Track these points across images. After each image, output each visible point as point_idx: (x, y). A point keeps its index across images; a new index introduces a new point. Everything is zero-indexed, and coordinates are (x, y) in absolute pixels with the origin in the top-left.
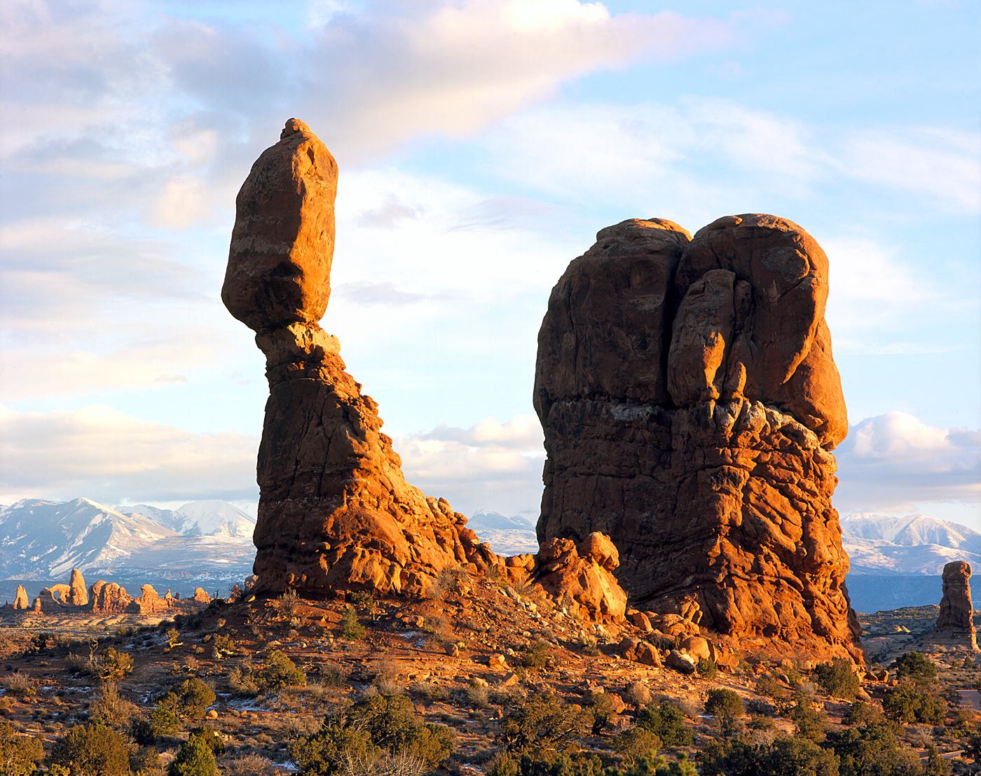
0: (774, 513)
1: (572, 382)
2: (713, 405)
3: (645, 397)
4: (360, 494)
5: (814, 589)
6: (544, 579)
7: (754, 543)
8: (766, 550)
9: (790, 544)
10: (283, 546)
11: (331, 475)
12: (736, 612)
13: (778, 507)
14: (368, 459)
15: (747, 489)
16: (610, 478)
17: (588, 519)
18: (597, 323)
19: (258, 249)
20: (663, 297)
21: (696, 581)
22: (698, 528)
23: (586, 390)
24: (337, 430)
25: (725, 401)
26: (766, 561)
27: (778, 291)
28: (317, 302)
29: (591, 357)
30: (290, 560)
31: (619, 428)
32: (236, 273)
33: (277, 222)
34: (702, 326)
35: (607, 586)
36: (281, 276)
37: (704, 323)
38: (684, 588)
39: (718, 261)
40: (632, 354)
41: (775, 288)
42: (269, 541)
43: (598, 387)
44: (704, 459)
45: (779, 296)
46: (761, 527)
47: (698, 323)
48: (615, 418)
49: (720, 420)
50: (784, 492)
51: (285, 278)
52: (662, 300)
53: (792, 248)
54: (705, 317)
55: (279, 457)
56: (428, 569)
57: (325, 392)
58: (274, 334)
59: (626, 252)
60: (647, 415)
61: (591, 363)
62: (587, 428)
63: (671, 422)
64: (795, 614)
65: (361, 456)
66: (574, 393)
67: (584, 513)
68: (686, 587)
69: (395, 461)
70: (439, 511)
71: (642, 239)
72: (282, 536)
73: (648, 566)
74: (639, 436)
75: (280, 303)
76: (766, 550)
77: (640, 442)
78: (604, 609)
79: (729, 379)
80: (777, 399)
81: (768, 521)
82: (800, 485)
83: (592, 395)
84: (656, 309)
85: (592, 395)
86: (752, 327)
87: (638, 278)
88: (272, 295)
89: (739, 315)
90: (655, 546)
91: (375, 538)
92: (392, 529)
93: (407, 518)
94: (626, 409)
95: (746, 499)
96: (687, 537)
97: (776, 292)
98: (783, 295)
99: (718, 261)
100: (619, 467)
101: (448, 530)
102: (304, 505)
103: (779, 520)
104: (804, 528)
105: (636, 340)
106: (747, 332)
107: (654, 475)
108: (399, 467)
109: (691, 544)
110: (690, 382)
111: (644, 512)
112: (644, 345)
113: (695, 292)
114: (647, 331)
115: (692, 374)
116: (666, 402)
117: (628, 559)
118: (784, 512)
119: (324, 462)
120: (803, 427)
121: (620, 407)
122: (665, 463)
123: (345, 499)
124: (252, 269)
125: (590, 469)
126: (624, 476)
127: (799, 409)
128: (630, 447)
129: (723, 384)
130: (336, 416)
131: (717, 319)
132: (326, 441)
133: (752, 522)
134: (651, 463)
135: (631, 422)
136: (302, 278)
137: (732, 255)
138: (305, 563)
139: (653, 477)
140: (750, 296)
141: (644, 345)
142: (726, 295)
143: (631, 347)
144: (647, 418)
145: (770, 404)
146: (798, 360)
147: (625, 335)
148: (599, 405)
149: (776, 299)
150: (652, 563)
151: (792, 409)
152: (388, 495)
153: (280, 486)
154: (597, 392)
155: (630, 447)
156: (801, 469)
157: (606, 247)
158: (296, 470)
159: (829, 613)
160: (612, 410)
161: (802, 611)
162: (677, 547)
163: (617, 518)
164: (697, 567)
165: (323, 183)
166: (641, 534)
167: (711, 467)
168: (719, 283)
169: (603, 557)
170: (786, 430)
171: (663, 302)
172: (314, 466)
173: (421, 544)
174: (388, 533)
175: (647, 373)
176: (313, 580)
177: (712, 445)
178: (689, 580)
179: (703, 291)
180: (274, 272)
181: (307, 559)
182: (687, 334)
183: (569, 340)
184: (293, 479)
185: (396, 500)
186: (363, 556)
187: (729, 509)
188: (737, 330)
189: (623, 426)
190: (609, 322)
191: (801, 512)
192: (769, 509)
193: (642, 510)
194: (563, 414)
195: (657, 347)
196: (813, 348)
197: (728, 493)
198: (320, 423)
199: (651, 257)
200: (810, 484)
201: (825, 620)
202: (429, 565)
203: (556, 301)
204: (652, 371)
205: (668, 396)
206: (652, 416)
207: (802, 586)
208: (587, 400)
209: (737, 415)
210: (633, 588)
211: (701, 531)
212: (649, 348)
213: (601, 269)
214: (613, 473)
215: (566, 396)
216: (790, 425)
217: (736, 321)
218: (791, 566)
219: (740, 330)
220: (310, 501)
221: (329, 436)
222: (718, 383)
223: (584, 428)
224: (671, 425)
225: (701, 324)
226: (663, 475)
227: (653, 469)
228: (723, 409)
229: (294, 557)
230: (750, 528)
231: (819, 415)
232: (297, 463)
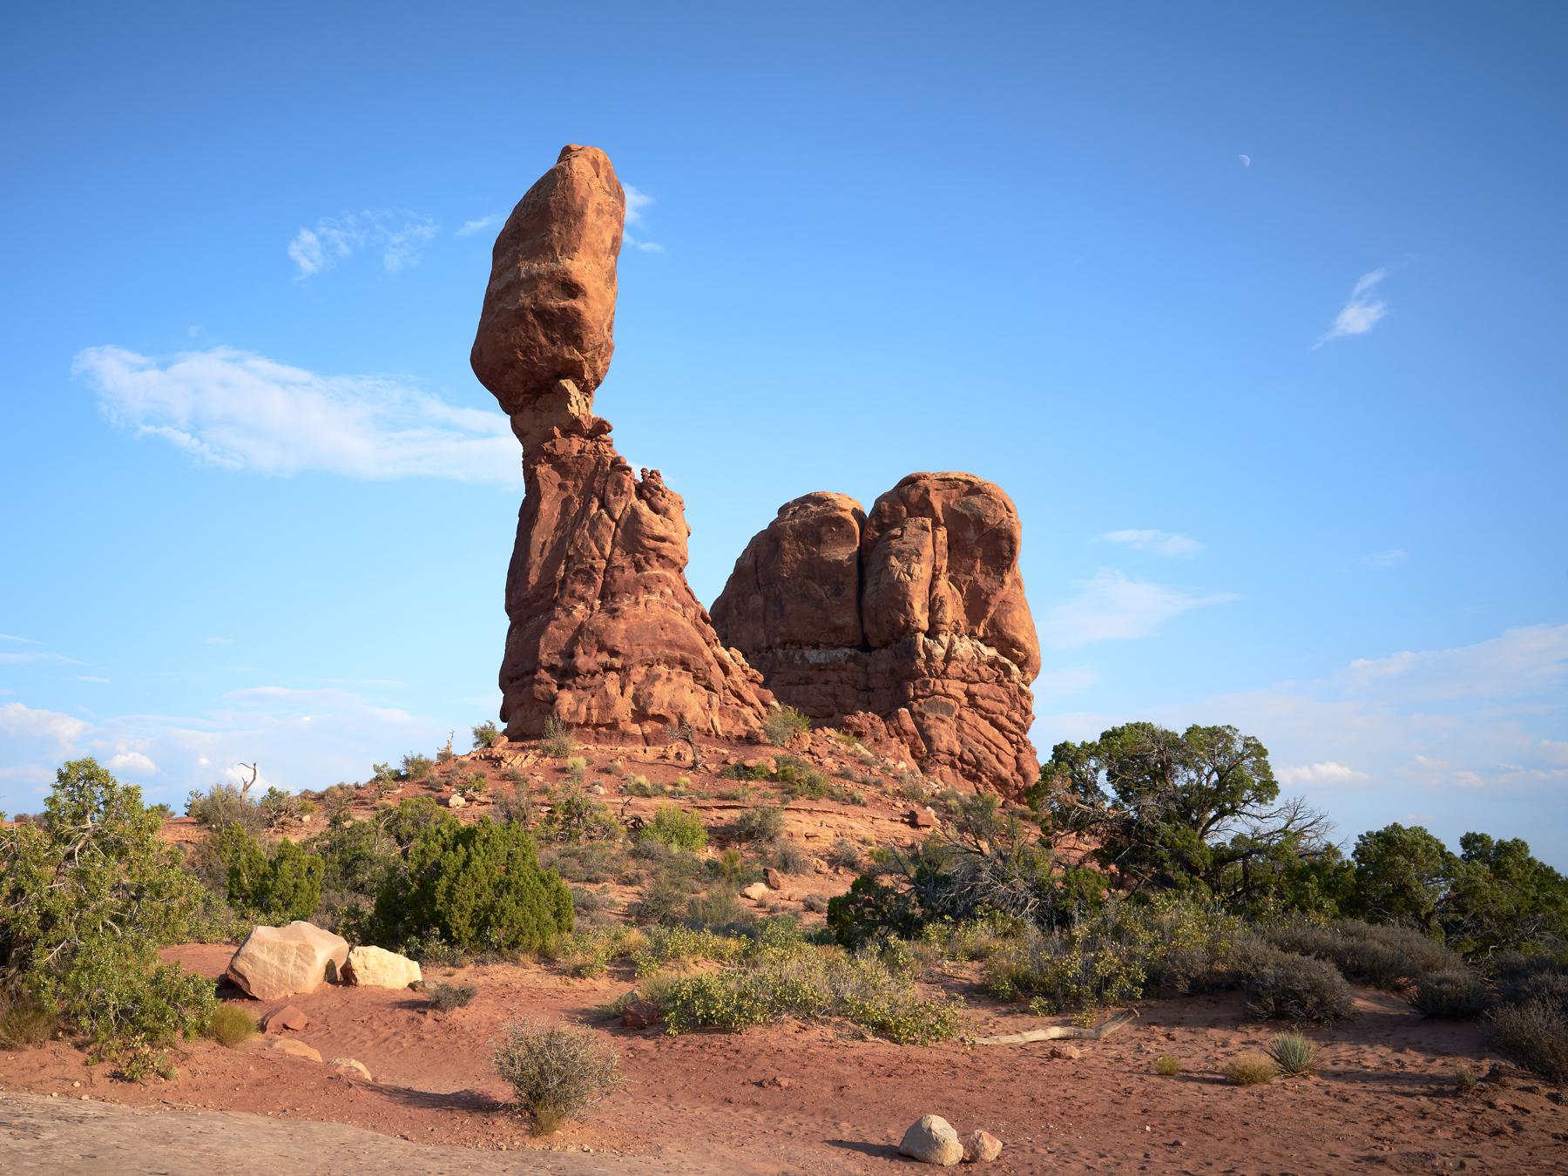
0: (987, 742)
1: (761, 635)
2: (921, 637)
4: (662, 593)
8: (985, 780)
9: (1005, 773)
14: (673, 543)
23: (778, 640)
25: (932, 633)
32: (492, 317)
41: (972, 531)
50: (994, 723)
58: (537, 404)
65: (663, 539)
76: (985, 780)
81: (981, 748)
82: (1008, 717)
83: (783, 645)
85: (783, 645)
91: (686, 654)
95: (960, 729)
103: (994, 749)
104: (1016, 758)
112: (838, 592)
113: (895, 537)
118: (997, 742)
120: (1007, 661)
121: (814, 652)
123: (642, 600)
133: (970, 751)
135: (827, 664)
136: (586, 303)
137: (924, 505)
141: (838, 592)
146: (1001, 594)
147: (816, 586)
148: (791, 653)
153: (542, 596)
156: (1007, 700)
160: (806, 655)
186: (669, 679)
187: (945, 738)
191: (1011, 742)
192: (983, 739)
196: (1013, 585)
197: (943, 721)
200: (1017, 717)
205: (865, 637)
209: (946, 646)
224: (867, 666)
230: (968, 756)
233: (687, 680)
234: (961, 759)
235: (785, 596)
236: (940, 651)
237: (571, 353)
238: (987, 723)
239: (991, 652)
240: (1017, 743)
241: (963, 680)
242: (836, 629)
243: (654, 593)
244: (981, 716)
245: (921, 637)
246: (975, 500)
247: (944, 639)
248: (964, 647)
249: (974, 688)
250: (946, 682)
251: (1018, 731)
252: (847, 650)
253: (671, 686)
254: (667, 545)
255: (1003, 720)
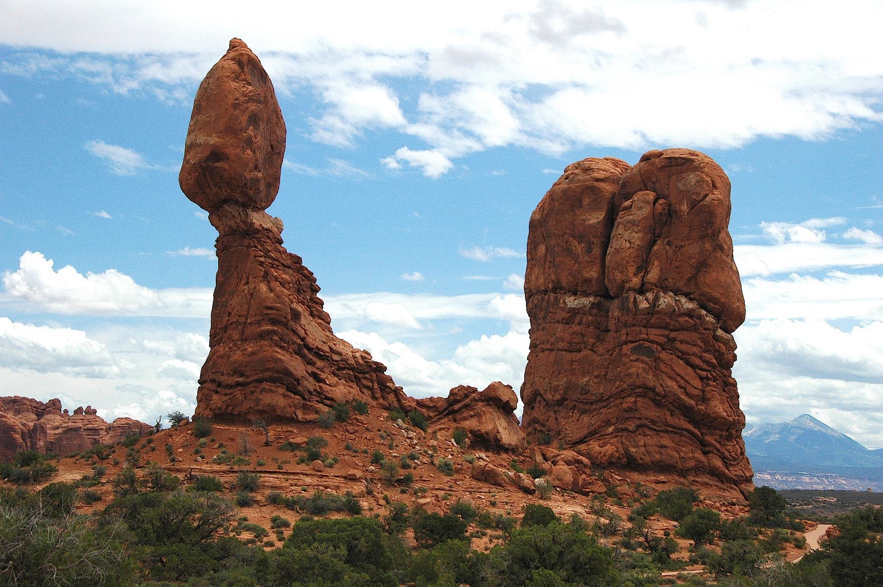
1: (542, 280)
3: (590, 290)
4: (271, 339)
5: (709, 438)
6: (450, 417)
7: (663, 401)
10: (213, 381)
11: (251, 323)
12: (644, 455)
13: (682, 373)
15: (657, 359)
16: (564, 352)
17: (550, 383)
18: (559, 235)
19: (198, 142)
20: (604, 214)
21: (617, 430)
22: (620, 389)
24: (257, 288)
26: (672, 415)
27: (687, 206)
28: (246, 184)
29: (554, 261)
30: (217, 392)
31: (571, 314)
33: (211, 118)
34: (628, 233)
35: (505, 424)
36: (214, 163)
37: (630, 231)
38: (606, 435)
39: (645, 185)
40: (581, 257)
41: (686, 205)
42: (206, 377)
43: (558, 284)
44: (627, 335)
45: (688, 210)
46: (668, 389)
47: (626, 231)
48: (568, 306)
49: (639, 306)
50: (688, 363)
51: (217, 164)
52: (601, 217)
53: (700, 173)
54: (630, 227)
55: (218, 311)
56: (328, 402)
57: (253, 258)
59: (580, 181)
60: (589, 303)
61: (554, 266)
62: (551, 314)
63: (608, 309)
64: (694, 458)
66: (542, 288)
67: (546, 379)
68: (609, 434)
69: (324, 317)
70: (361, 361)
71: (592, 171)
72: (213, 373)
73: (585, 419)
74: (584, 320)
75: (215, 185)
77: (586, 325)
78: (498, 441)
79: (648, 274)
80: (685, 290)
83: (555, 290)
84: (598, 222)
85: (555, 290)
86: (669, 235)
87: (587, 200)
88: (209, 178)
89: (657, 226)
90: (591, 403)
92: (297, 367)
93: (320, 364)
94: (576, 299)
96: (612, 396)
97: (686, 208)
98: (692, 209)
99: (645, 185)
100: (571, 344)
101: (367, 375)
102: (230, 348)
105: (584, 247)
106: (664, 238)
107: (595, 349)
108: (329, 323)
109: (614, 401)
110: (617, 276)
111: (585, 377)
114: (592, 240)
115: (619, 270)
116: (606, 295)
117: (573, 413)
118: (687, 378)
119: (247, 314)
120: (704, 312)
121: (572, 298)
122: (603, 340)
124: (194, 158)
125: (552, 345)
126: (574, 350)
127: (702, 298)
128: (577, 328)
129: (643, 278)
130: (258, 277)
131: (639, 228)
132: (249, 297)
133: (661, 385)
134: (592, 341)
137: (655, 180)
138: (226, 395)
139: (594, 351)
140: (667, 211)
141: (589, 250)
142: (646, 211)
143: (580, 252)
144: (590, 305)
145: (680, 294)
148: (559, 297)
149: (686, 213)
150: (589, 416)
151: (697, 297)
152: (299, 341)
154: (557, 288)
155: (577, 328)
156: (702, 345)
157: (566, 179)
158: (228, 320)
159: (724, 458)
160: (566, 301)
161: (699, 455)
162: (605, 404)
163: (566, 382)
164: (617, 419)
165: (250, 88)
166: (582, 395)
167: (632, 342)
168: (643, 201)
169: (500, 400)
170: (690, 314)
171: (604, 218)
172: (240, 316)
173: (327, 383)
174: (292, 369)
175: (590, 271)
176: (230, 408)
177: (633, 325)
178: (611, 429)
179: (631, 207)
180: (208, 159)
181: (228, 391)
182: (617, 240)
183: (542, 249)
184: (226, 328)
185: (307, 346)
188: (656, 237)
189: (574, 312)
190: (567, 234)
191: (701, 379)
192: (674, 376)
193: (584, 376)
194: (535, 305)
195: (598, 252)
197: (643, 362)
198: (247, 283)
199: (596, 184)
200: (707, 356)
201: (718, 463)
202: (332, 399)
203: (534, 221)
204: (594, 270)
205: (607, 289)
206: (593, 304)
207: (701, 436)
208: (552, 293)
209: (651, 301)
210: (571, 435)
211: (622, 391)
212: (593, 253)
213: (562, 195)
214: (566, 348)
215: (538, 291)
216: (693, 310)
217: (655, 230)
218: (691, 421)
219: (659, 237)
220: (235, 345)
221: (251, 292)
222: (639, 278)
223: (548, 315)
225: (627, 232)
226: (600, 349)
227: (594, 344)
228: (641, 297)
229: (219, 389)
230: (659, 389)
231: (716, 301)
232: (230, 314)
233: (281, 390)
234: (653, 390)
235: (556, 249)
236: (644, 305)
237: (226, 190)
238: (681, 362)
239: (688, 305)
240: (707, 378)
241: (665, 328)
242: (587, 281)
243: (266, 340)
244: (678, 357)
245: (632, 295)
246: (692, 178)
247: (650, 295)
248: (666, 300)
249: (673, 335)
250: (650, 330)
251: (709, 369)
252: (591, 299)
253: (269, 395)
254: (274, 312)
255: (697, 362)
